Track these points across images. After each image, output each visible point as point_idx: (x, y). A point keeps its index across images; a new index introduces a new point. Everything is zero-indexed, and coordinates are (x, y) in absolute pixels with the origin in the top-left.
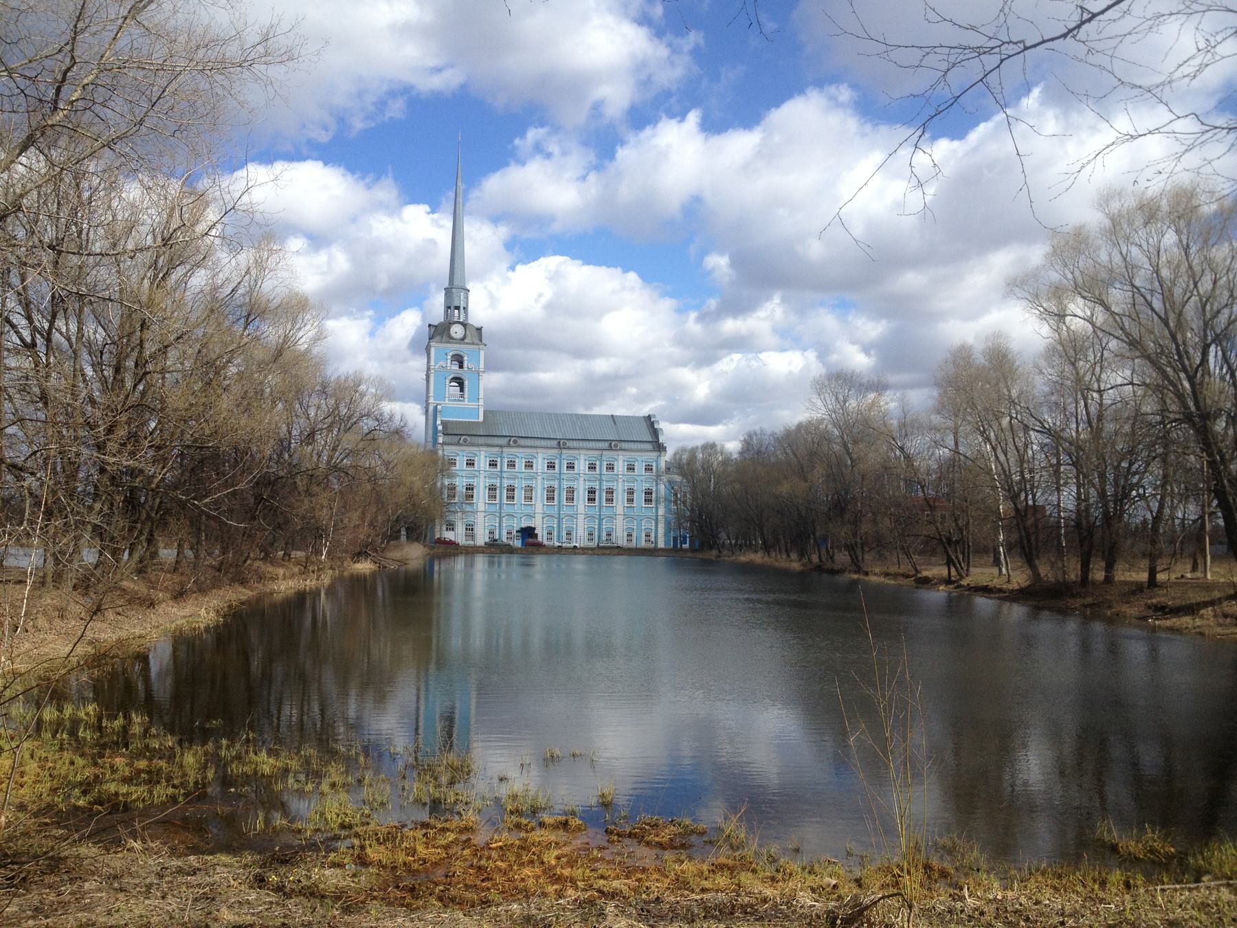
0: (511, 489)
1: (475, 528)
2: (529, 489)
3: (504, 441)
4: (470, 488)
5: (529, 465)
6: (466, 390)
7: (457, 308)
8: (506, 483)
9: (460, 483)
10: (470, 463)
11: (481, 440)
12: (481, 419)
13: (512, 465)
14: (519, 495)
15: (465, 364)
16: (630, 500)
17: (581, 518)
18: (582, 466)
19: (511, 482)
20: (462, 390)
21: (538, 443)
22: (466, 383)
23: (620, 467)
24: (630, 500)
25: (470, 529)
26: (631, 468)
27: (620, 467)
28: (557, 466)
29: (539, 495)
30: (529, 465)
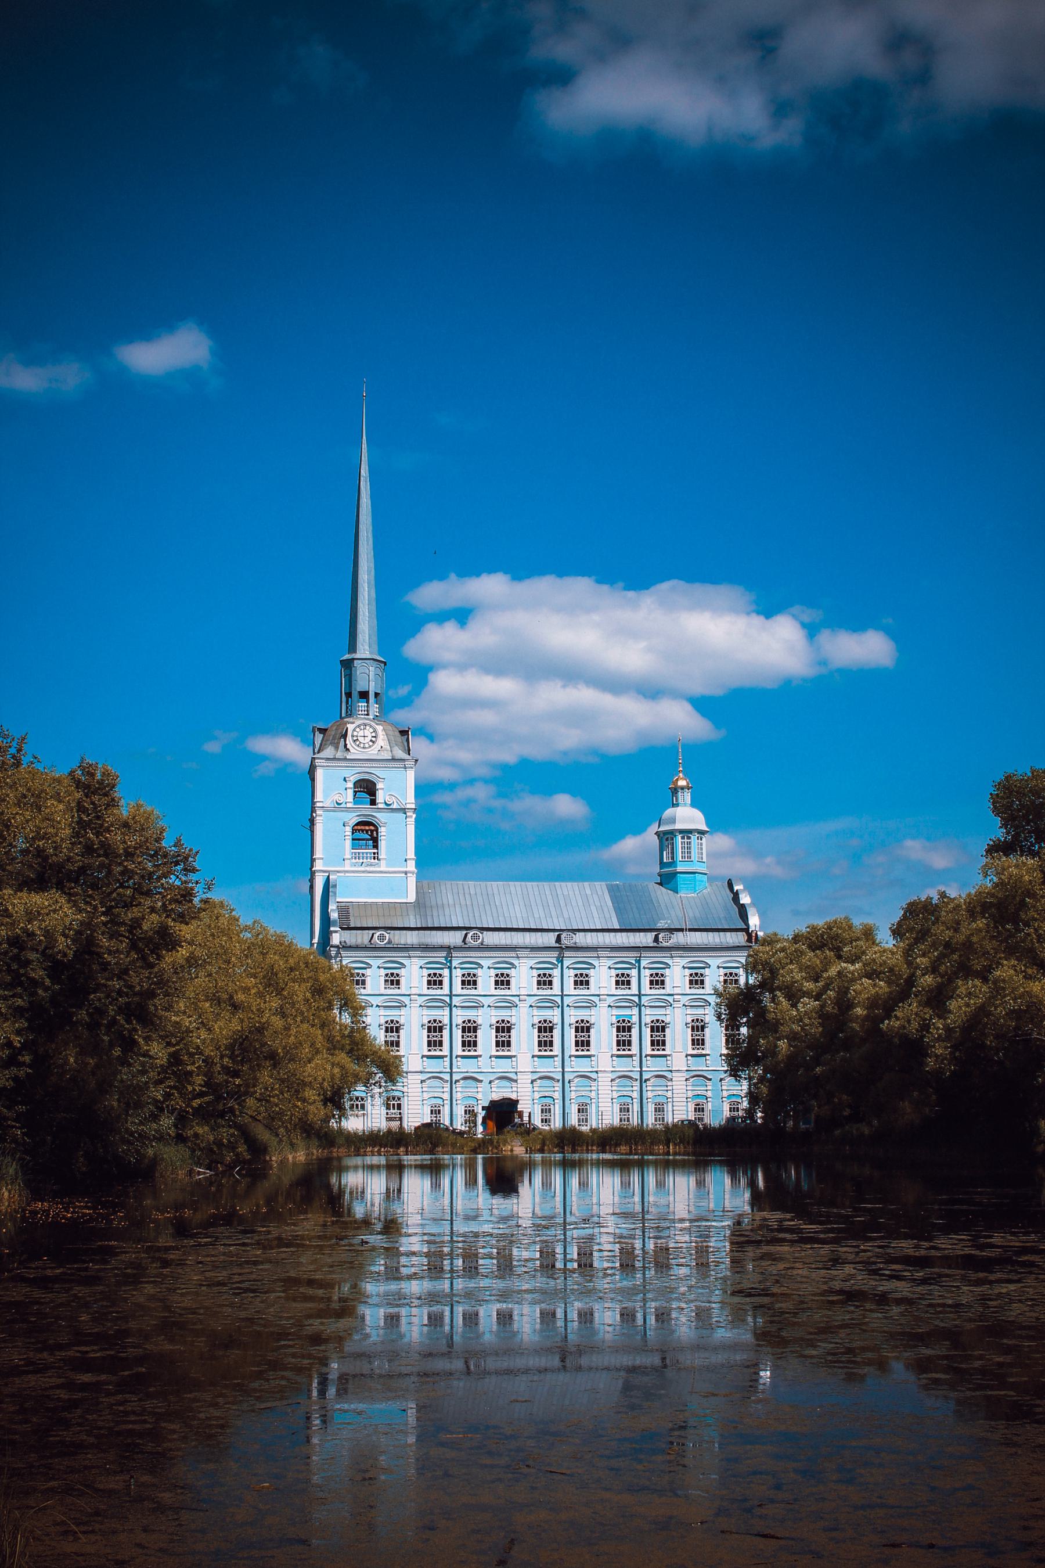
0: (470, 1028)
1: (404, 1102)
2: (504, 1029)
3: (454, 938)
4: (393, 1028)
5: (503, 982)
6: (382, 844)
7: (364, 695)
8: (460, 1016)
9: (374, 1022)
10: (393, 981)
11: (411, 938)
12: (412, 898)
13: (470, 982)
14: (486, 1038)
15: (380, 797)
16: (698, 1042)
17: (604, 1080)
18: (603, 977)
19: (470, 1014)
20: (376, 847)
21: (518, 939)
22: (382, 831)
23: (677, 975)
24: (698, 1042)
25: (393, 1104)
26: (697, 981)
27: (677, 975)
28: (556, 982)
29: (524, 1039)
30: (503, 982)
